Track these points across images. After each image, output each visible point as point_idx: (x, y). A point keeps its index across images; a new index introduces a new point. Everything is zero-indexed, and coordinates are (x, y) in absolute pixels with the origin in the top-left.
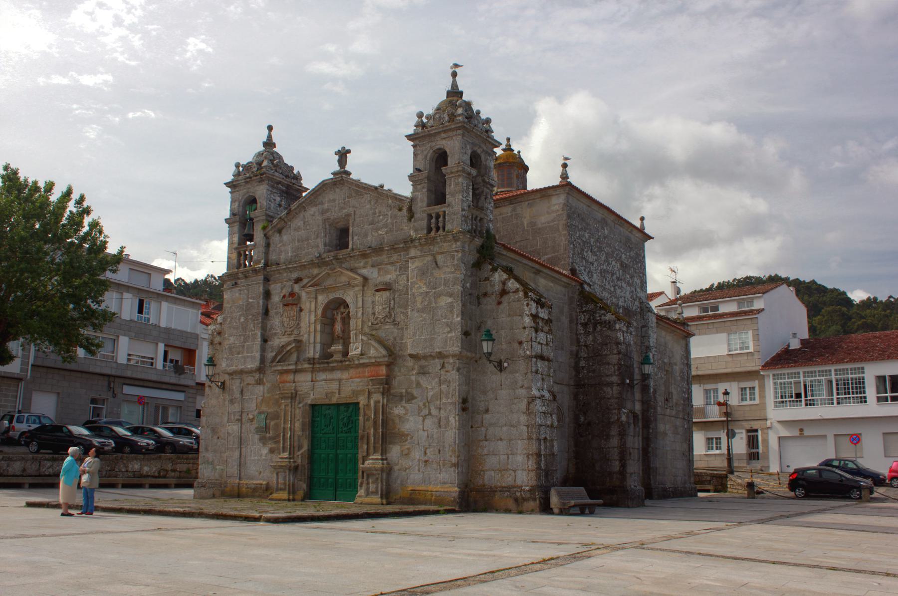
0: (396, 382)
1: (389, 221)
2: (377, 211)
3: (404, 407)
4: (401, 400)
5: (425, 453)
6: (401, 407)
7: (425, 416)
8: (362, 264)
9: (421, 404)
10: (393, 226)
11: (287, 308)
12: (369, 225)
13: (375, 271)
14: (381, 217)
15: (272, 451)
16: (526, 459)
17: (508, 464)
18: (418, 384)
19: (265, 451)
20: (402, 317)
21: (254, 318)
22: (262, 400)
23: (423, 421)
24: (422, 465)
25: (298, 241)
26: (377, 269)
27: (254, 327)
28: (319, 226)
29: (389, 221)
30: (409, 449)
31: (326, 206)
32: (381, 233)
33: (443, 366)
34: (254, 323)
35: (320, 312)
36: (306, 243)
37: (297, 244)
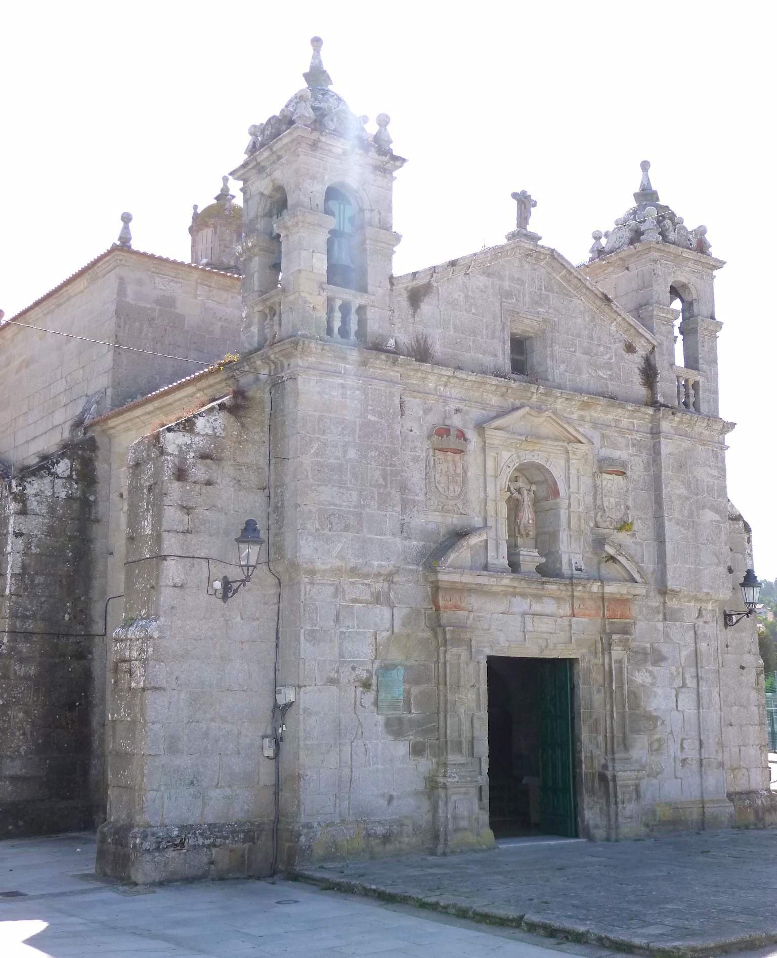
0: (637, 630)
2: (595, 336)
3: (650, 672)
4: (645, 661)
5: (682, 748)
9: (673, 669)
10: (619, 370)
11: (440, 455)
14: (602, 349)
15: (417, 750)
16: (759, 752)
17: (740, 759)
19: (402, 748)
21: (382, 459)
22: (388, 639)
23: (677, 697)
24: (678, 765)
26: (599, 434)
27: (385, 479)
30: (659, 740)
31: (506, 284)
32: (601, 374)
37: (452, 332)
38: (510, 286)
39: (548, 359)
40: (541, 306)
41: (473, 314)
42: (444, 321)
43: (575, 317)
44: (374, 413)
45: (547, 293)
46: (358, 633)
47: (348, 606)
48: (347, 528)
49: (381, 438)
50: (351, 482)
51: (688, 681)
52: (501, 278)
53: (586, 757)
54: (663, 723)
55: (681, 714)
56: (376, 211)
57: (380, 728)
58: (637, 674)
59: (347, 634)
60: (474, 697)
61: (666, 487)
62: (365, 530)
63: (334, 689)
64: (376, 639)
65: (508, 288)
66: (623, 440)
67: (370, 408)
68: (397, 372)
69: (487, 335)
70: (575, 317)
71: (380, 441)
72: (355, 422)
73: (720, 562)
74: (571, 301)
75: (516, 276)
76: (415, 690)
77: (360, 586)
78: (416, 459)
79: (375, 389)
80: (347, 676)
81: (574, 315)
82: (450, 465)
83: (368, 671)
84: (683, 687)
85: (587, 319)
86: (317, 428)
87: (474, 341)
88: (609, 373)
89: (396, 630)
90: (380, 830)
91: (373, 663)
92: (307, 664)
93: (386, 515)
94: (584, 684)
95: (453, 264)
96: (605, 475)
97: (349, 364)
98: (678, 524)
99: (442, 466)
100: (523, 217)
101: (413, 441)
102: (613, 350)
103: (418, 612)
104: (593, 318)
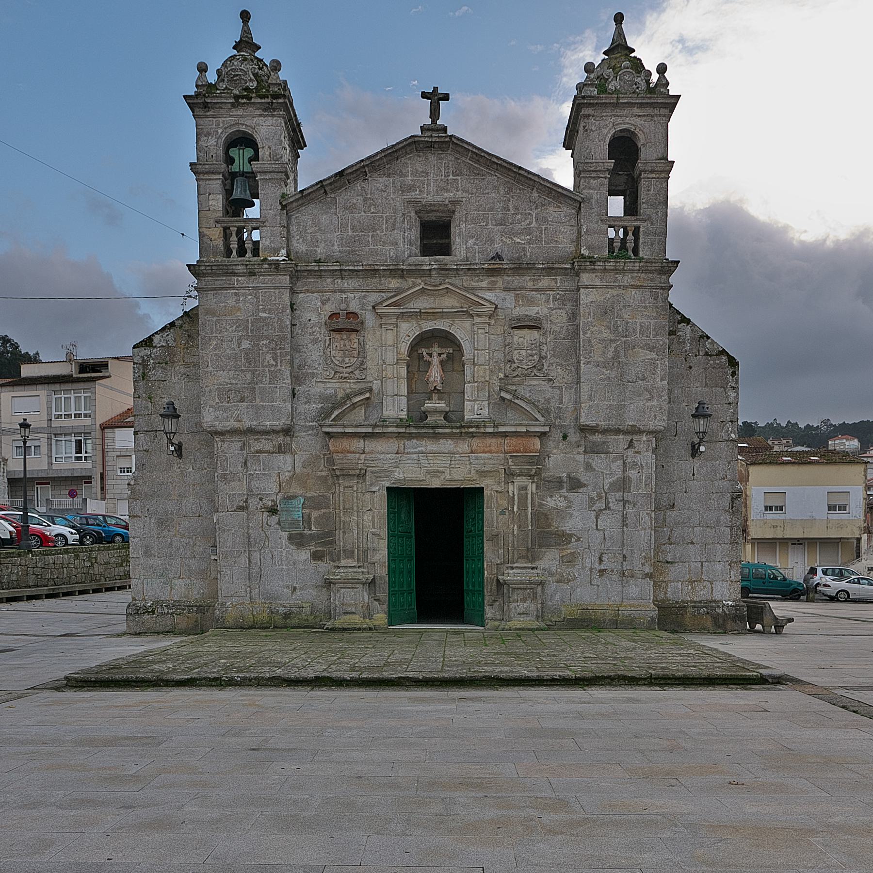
1: (534, 224)
2: (511, 205)
4: (561, 487)
5: (601, 560)
7: (601, 510)
8: (484, 284)
9: (594, 495)
10: (541, 233)
11: (337, 336)
12: (497, 225)
13: (510, 297)
14: (519, 216)
15: (317, 556)
18: (588, 467)
19: (304, 555)
20: (559, 370)
21: (273, 345)
22: (291, 477)
23: (597, 517)
24: (595, 575)
25: (353, 228)
26: (513, 295)
27: (275, 360)
28: (395, 210)
29: (534, 224)
32: (519, 240)
33: (631, 445)
34: (276, 354)
35: (404, 348)
36: (370, 234)
37: (350, 233)
39: (457, 238)
41: (372, 213)
42: (342, 225)
43: (488, 193)
46: (264, 474)
48: (242, 400)
49: (271, 329)
50: (245, 366)
51: (611, 505)
53: (487, 565)
54: (578, 540)
55: (602, 532)
56: (267, 147)
57: (284, 541)
59: (255, 475)
60: (370, 518)
61: (584, 333)
62: (258, 400)
63: (244, 514)
67: (261, 307)
69: (387, 228)
71: (271, 331)
73: (652, 397)
74: (484, 179)
75: (420, 170)
76: (315, 514)
77: (263, 440)
78: (315, 341)
79: (266, 292)
80: (253, 503)
83: (273, 501)
84: (605, 509)
86: (215, 330)
88: (528, 237)
89: (297, 471)
90: (281, 610)
91: (277, 494)
92: (220, 497)
93: (277, 387)
94: (487, 508)
95: (341, 174)
96: (517, 332)
98: (598, 366)
100: (435, 113)
102: (534, 216)
103: (318, 457)
104: (511, 189)
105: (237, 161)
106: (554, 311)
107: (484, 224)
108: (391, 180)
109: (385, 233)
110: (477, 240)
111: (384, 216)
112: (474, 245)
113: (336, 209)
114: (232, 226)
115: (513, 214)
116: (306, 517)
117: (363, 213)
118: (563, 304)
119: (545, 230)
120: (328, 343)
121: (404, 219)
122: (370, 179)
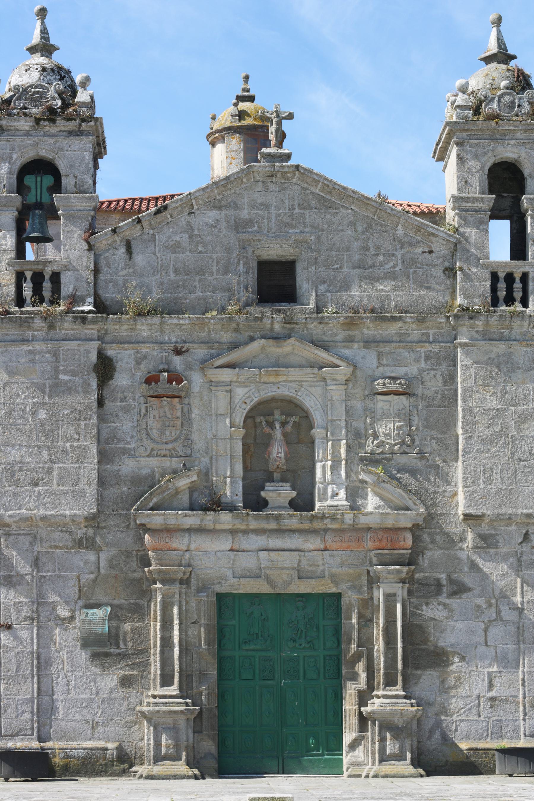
2: (371, 245)
3: (445, 605)
6: (439, 604)
7: (490, 621)
12: (354, 268)
14: (381, 258)
20: (434, 445)
22: (95, 580)
23: (486, 631)
25: (177, 271)
26: (375, 353)
28: (228, 250)
31: (245, 214)
32: (382, 287)
34: (79, 426)
35: (239, 419)
37: (172, 276)
38: (249, 214)
39: (305, 282)
40: (293, 227)
42: (162, 266)
43: (342, 230)
44: (65, 372)
45: (302, 211)
46: (59, 576)
47: (48, 552)
52: (236, 207)
58: (424, 608)
59: (47, 577)
64: (79, 581)
65: (247, 217)
66: (412, 354)
67: (61, 368)
68: (92, 329)
69: (218, 271)
70: (342, 230)
72: (44, 385)
74: (337, 213)
75: (259, 201)
81: (340, 228)
82: (167, 409)
85: (360, 229)
87: (200, 281)
89: (103, 571)
91: (76, 602)
97: (37, 330)
99: (156, 413)
101: (123, 392)
102: (399, 257)
104: (369, 227)
105: (33, 191)
106: (426, 373)
107: (339, 266)
108: (223, 213)
109: (215, 276)
110: (329, 286)
111: (215, 256)
112: (326, 292)
113: (155, 248)
114: (27, 270)
115: (374, 255)
116: (113, 631)
117: (188, 253)
118: (437, 363)
119: (413, 273)
120: (143, 411)
121: (239, 260)
122: (197, 212)
